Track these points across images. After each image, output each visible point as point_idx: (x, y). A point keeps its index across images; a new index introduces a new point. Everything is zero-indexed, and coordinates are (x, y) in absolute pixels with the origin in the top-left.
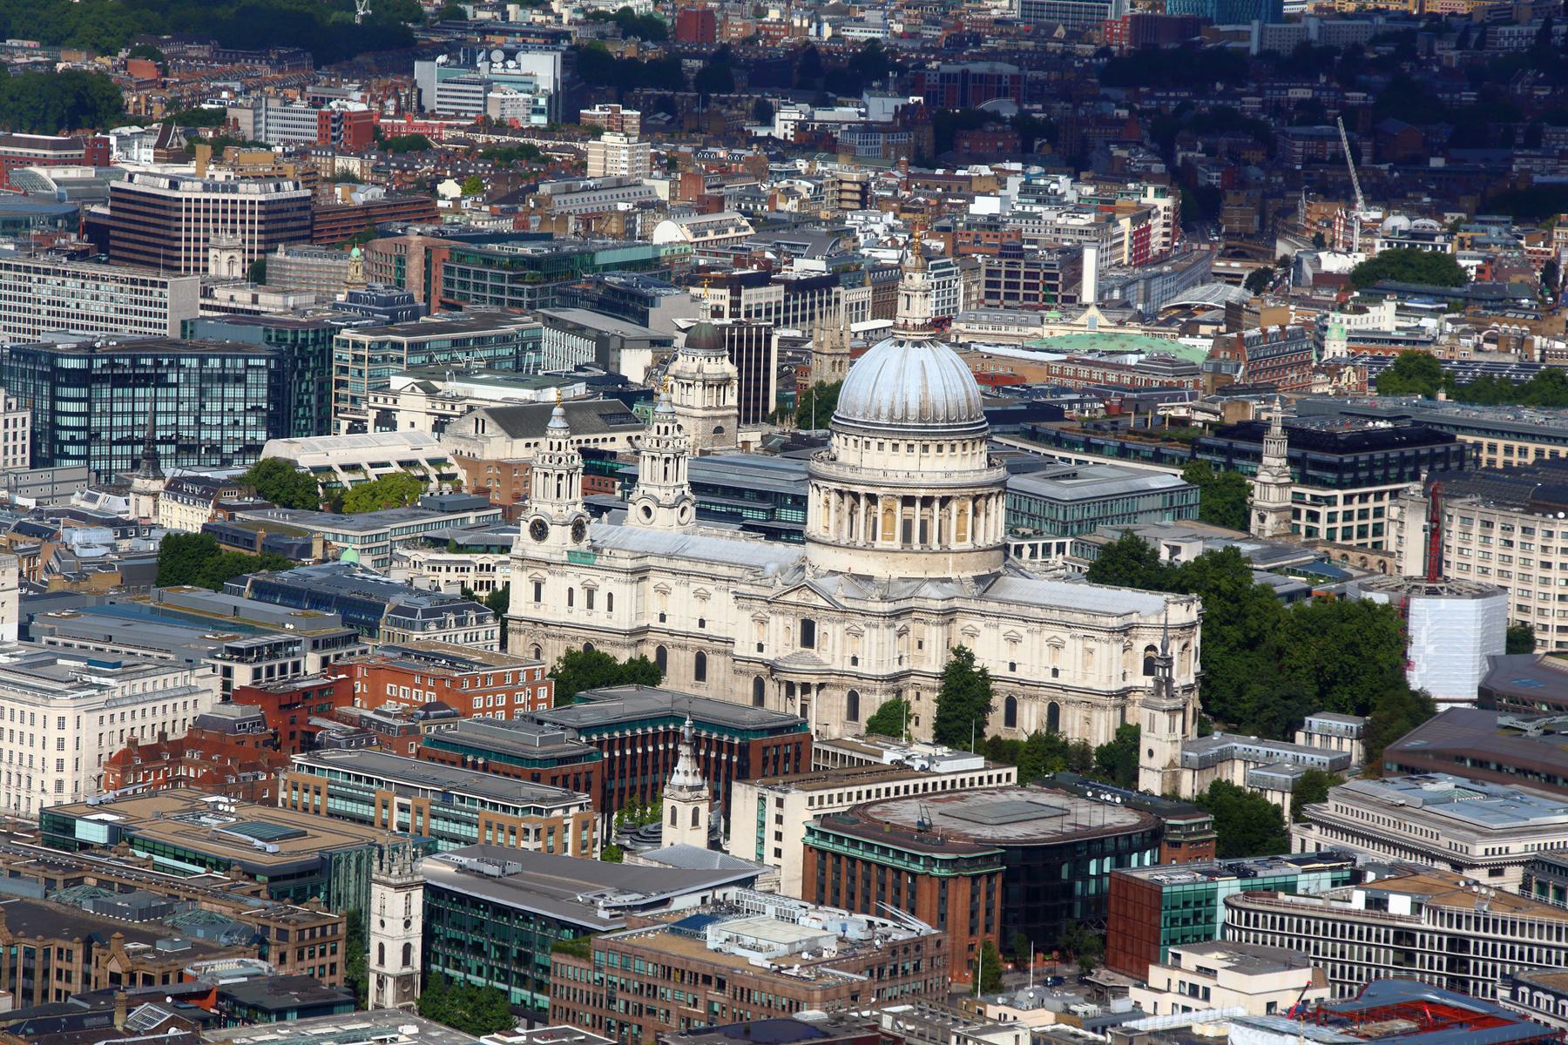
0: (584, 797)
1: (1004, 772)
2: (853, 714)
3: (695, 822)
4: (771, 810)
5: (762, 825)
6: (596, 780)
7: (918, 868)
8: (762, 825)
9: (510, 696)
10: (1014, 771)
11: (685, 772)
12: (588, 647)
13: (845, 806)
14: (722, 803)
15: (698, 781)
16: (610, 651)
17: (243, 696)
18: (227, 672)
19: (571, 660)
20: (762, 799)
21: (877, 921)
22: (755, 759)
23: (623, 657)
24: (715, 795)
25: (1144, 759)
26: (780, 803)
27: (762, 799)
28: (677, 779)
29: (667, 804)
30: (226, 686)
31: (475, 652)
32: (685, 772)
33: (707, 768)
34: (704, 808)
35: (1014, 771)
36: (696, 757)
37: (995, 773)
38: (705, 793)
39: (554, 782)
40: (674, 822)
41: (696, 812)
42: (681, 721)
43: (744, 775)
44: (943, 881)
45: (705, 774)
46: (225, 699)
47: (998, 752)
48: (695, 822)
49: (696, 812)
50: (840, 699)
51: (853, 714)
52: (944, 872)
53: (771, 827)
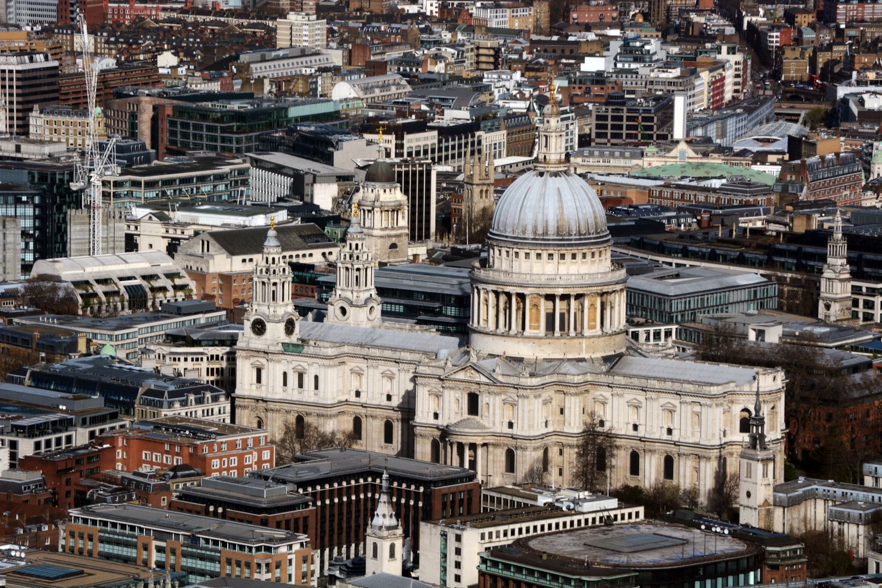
1: (633, 510)
3: (392, 555)
4: (452, 544)
9: (241, 457)
10: (641, 510)
11: (384, 515)
15: (393, 522)
17: (27, 464)
18: (13, 445)
20: (444, 535)
22: (437, 505)
25: (743, 499)
26: (458, 538)
27: (444, 535)
28: (378, 521)
29: (370, 541)
30: (13, 456)
32: (384, 515)
33: (399, 512)
34: (399, 543)
35: (641, 510)
36: (390, 502)
37: (626, 511)
38: (400, 531)
39: (278, 526)
40: (375, 555)
41: (392, 547)
43: (428, 517)
45: (398, 516)
46: (12, 466)
48: (392, 555)
49: (392, 547)
50: (500, 455)
53: (452, 558)
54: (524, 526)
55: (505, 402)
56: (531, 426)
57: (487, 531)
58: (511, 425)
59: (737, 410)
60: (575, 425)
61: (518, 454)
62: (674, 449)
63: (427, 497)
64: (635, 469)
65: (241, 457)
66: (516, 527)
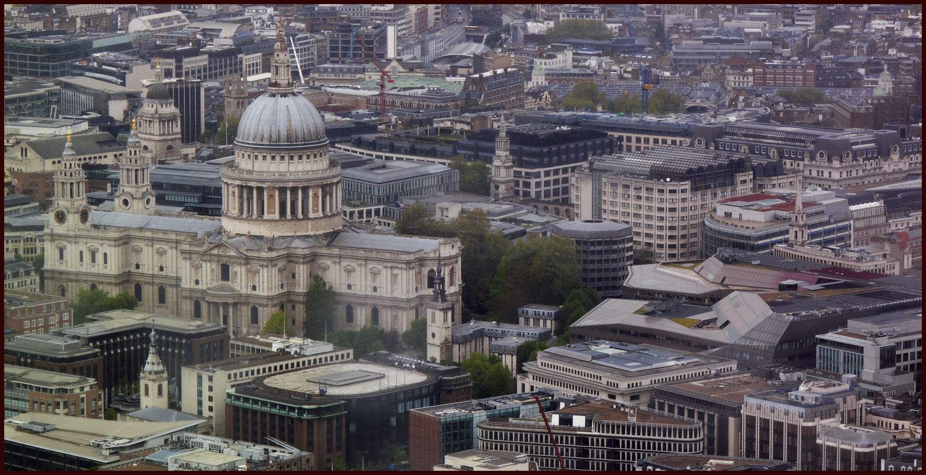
0: (92, 381)
1: (345, 352)
2: (255, 318)
3: (160, 393)
4: (206, 383)
5: (200, 393)
6: (100, 368)
7: (294, 415)
8: (200, 393)
9: (46, 319)
10: (351, 351)
12: (93, 287)
13: (250, 378)
14: (175, 379)
15: (161, 368)
16: (107, 288)
19: (82, 295)
20: (200, 378)
21: (270, 448)
23: (114, 292)
24: (171, 375)
25: (430, 339)
26: (210, 379)
27: (200, 378)
28: (148, 367)
29: (142, 383)
31: (23, 294)
32: (152, 363)
34: (165, 384)
35: (351, 351)
37: (340, 353)
38: (165, 375)
39: (74, 372)
40: (147, 393)
41: (160, 387)
42: (149, 330)
43: (190, 363)
44: (310, 422)
47: (341, 342)
49: (160, 387)
50: (246, 311)
51: (255, 318)
52: (310, 417)
53: (206, 394)
54: (261, 367)
55: (249, 271)
56: (270, 289)
57: (232, 372)
58: (254, 288)
59: (425, 271)
60: (302, 286)
61: (260, 309)
62: (379, 302)
63: (189, 347)
64: (350, 317)
65: (46, 319)
66: (255, 368)
